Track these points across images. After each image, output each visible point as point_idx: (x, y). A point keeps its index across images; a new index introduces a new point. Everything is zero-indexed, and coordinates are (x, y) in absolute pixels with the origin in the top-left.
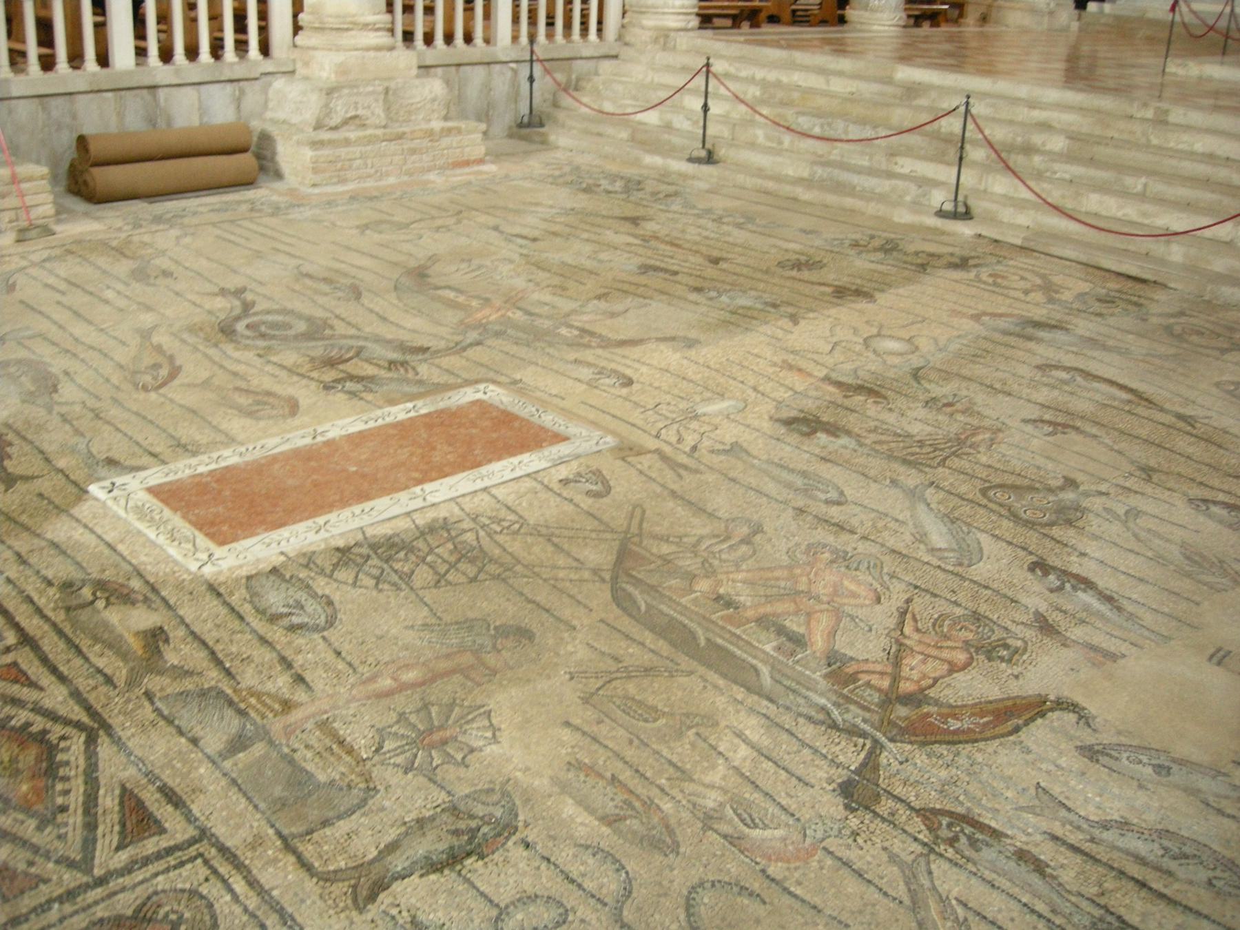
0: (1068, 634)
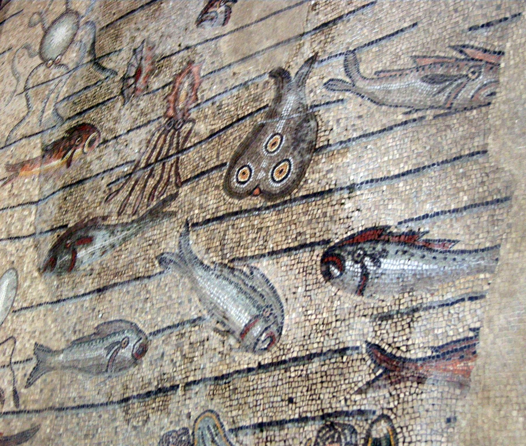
0: (411, 355)
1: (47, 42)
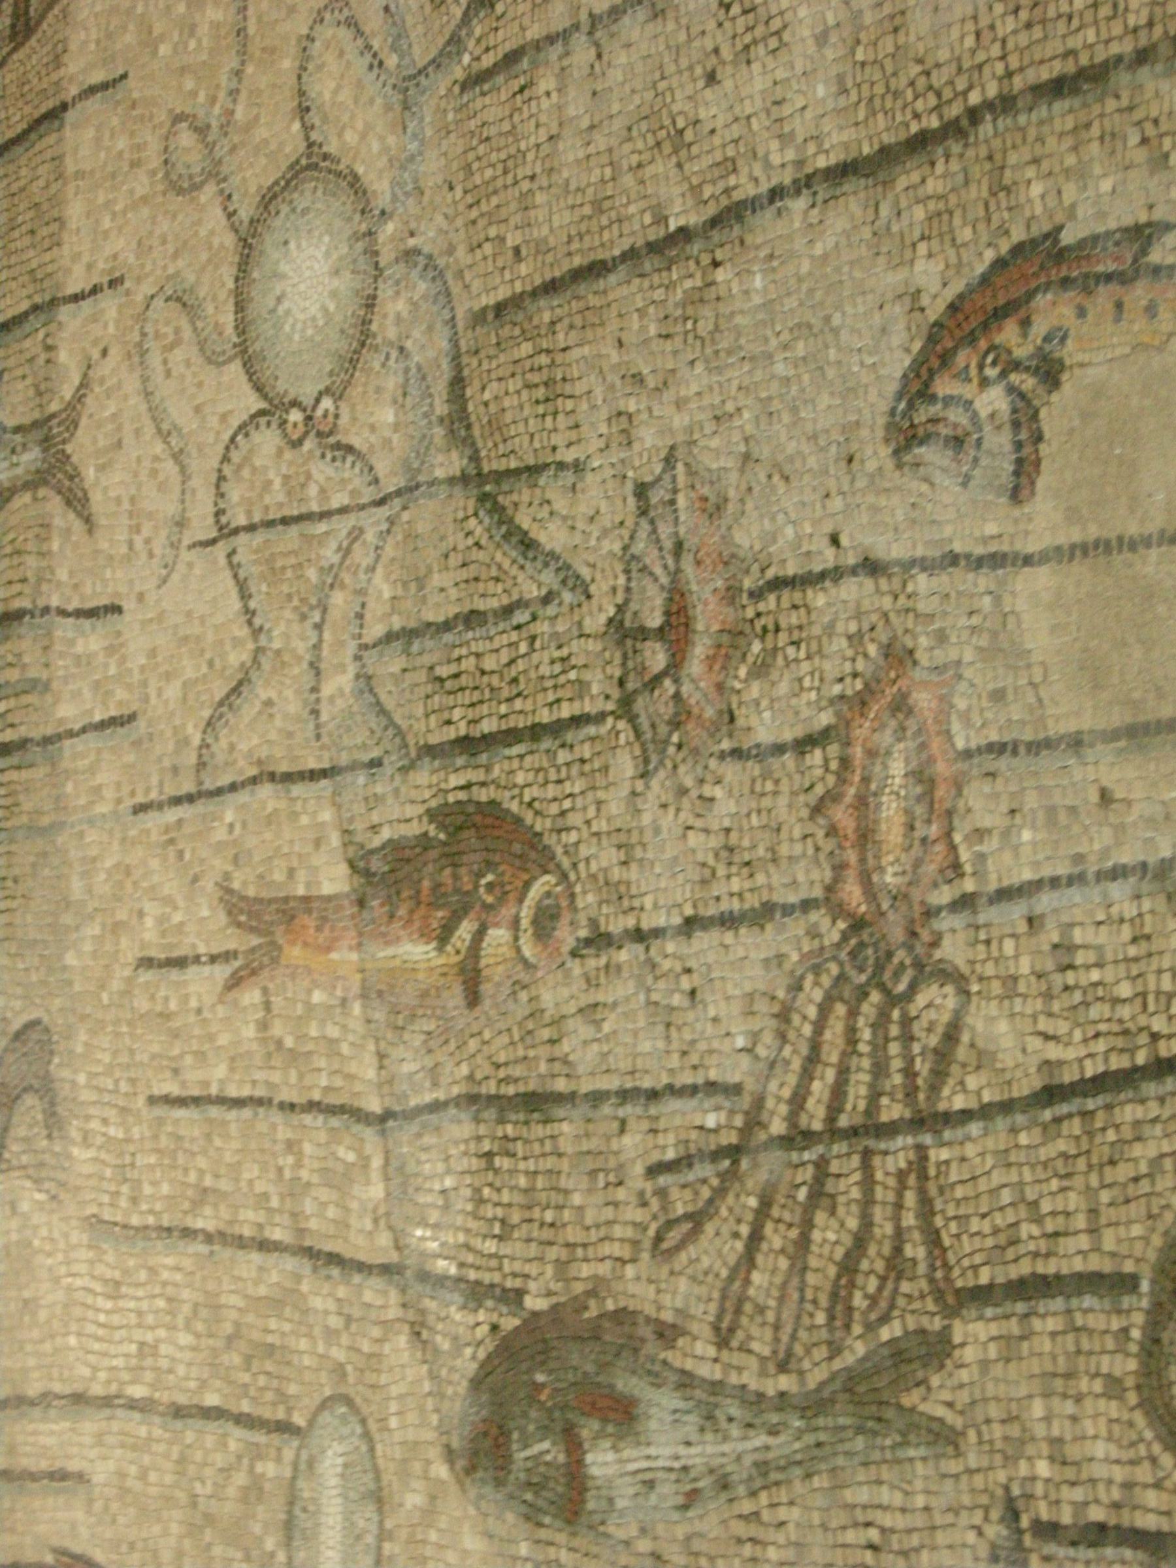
1: (261, 303)
